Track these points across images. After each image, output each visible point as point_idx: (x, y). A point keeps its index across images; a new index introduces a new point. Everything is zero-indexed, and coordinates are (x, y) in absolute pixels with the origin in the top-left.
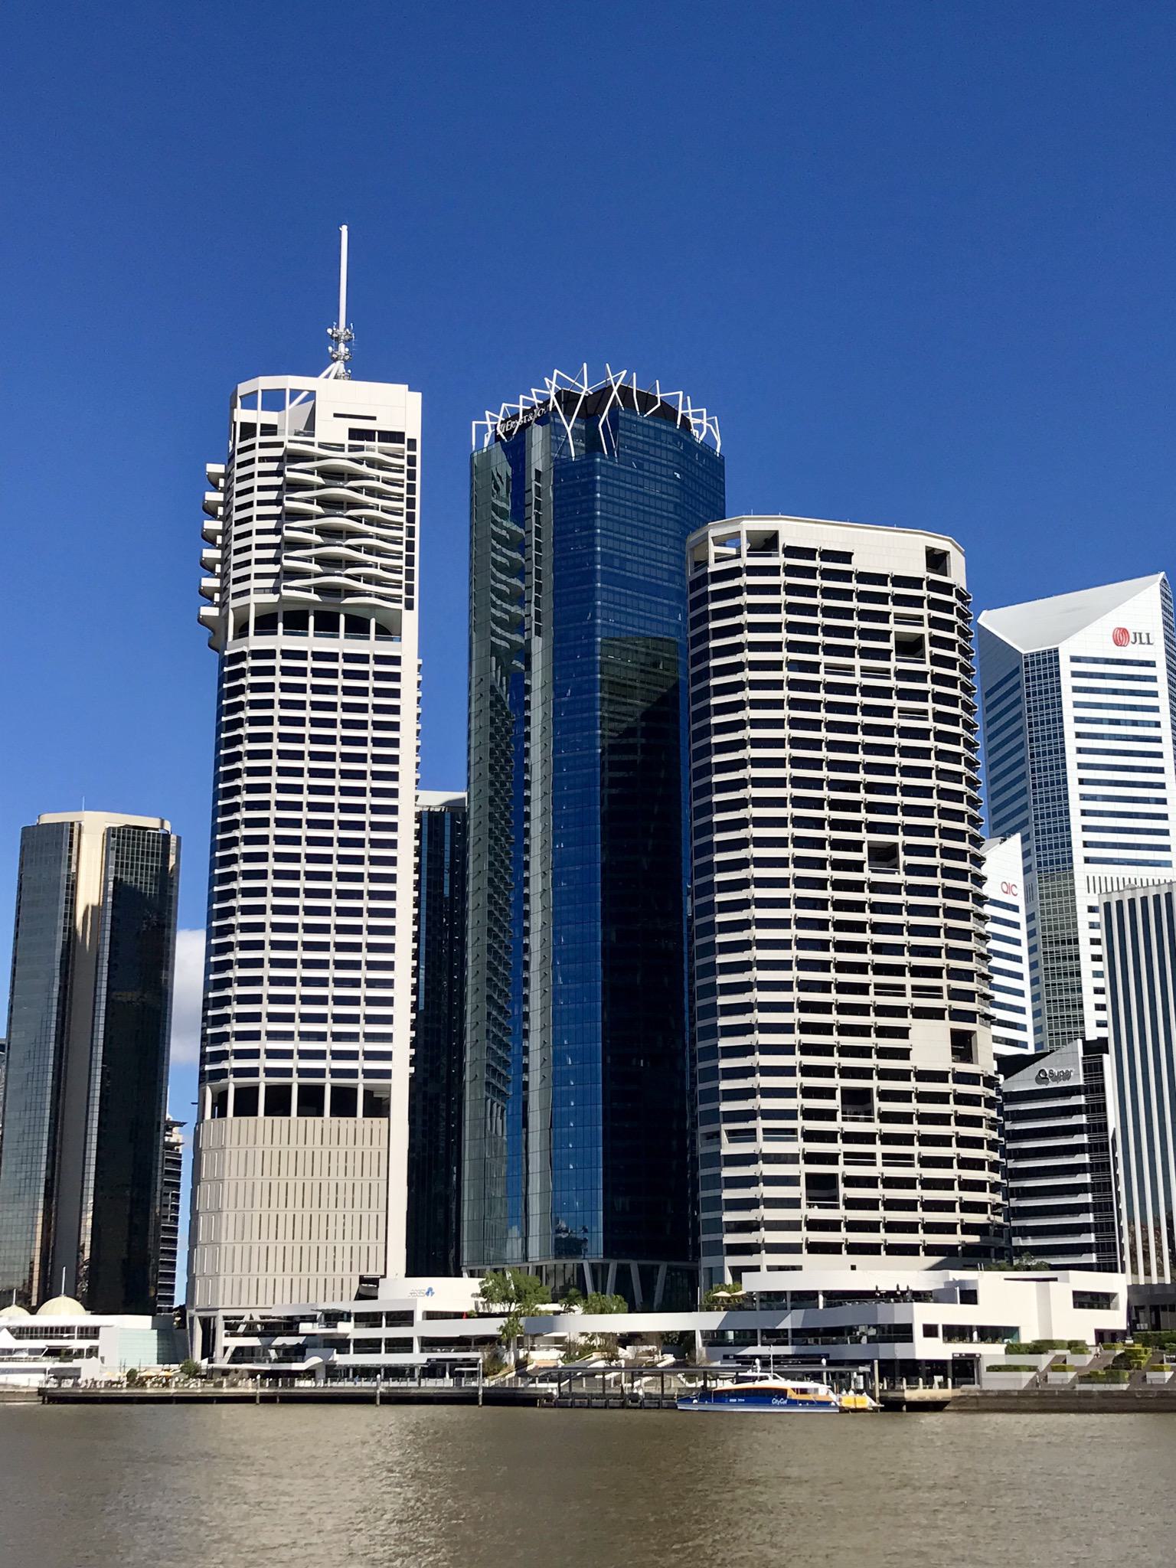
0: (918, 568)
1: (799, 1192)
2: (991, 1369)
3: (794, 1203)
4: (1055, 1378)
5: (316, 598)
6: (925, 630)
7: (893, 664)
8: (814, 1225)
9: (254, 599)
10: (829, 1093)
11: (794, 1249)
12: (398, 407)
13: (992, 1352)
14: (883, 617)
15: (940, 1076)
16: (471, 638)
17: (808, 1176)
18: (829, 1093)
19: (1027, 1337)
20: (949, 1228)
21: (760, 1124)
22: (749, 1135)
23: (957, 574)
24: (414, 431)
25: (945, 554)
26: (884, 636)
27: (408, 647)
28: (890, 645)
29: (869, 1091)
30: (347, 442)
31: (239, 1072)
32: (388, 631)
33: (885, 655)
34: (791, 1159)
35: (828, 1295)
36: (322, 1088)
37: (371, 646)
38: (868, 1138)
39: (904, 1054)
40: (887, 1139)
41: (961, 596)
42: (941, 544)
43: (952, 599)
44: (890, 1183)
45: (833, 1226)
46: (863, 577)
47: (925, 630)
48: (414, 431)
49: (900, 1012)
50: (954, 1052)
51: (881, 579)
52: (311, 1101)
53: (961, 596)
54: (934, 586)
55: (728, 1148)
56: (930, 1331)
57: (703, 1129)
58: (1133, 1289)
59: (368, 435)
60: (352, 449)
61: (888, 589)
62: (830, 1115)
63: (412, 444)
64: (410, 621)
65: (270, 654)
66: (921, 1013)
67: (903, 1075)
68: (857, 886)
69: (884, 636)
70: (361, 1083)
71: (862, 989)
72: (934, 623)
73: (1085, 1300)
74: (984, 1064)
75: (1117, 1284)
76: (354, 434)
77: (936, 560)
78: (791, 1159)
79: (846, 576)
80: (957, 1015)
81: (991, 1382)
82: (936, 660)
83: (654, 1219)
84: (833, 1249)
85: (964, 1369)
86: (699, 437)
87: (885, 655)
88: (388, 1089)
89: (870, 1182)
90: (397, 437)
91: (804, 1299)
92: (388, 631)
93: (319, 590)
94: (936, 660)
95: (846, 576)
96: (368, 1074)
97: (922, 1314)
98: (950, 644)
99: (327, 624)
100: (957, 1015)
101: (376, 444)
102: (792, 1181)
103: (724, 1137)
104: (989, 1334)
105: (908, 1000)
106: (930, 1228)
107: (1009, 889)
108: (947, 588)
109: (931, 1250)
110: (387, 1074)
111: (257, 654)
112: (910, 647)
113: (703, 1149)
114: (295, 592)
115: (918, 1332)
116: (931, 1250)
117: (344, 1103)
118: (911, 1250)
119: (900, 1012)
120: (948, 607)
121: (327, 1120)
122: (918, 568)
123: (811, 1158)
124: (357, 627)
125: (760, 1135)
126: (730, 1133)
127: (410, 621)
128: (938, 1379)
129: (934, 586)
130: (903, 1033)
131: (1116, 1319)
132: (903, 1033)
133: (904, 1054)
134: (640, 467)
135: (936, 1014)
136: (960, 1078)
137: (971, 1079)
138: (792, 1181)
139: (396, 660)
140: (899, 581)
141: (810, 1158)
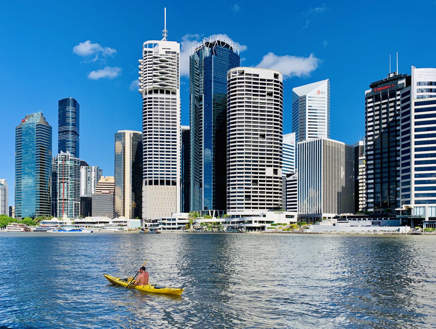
1: (244, 198)
2: (268, 228)
3: (243, 200)
5: (160, 87)
6: (273, 91)
8: (246, 204)
9: (148, 87)
10: (250, 181)
11: (243, 208)
14: (265, 88)
15: (271, 177)
16: (190, 94)
17: (245, 195)
18: (250, 181)
20: (271, 204)
21: (237, 186)
26: (265, 92)
27: (178, 96)
28: (266, 94)
29: (257, 180)
31: (149, 178)
33: (264, 96)
34: (243, 192)
36: (164, 180)
37: (171, 96)
38: (257, 189)
40: (260, 189)
41: (281, 83)
42: (277, 73)
43: (279, 84)
44: (260, 196)
45: (250, 204)
50: (274, 173)
52: (162, 183)
53: (281, 83)
54: (275, 81)
55: (231, 190)
57: (227, 187)
58: (298, 215)
62: (250, 185)
64: (178, 91)
65: (151, 98)
67: (264, 177)
68: (257, 142)
69: (265, 92)
70: (171, 180)
71: (257, 162)
72: (275, 89)
73: (287, 216)
74: (280, 175)
75: (296, 214)
78: (243, 192)
82: (275, 97)
83: (221, 204)
84: (250, 208)
85: (263, 228)
86: (235, 51)
87: (264, 96)
88: (176, 181)
89: (257, 196)
91: (238, 216)
92: (174, 93)
93: (160, 85)
94: (275, 97)
96: (172, 178)
97: (253, 219)
98: (278, 93)
99: (162, 92)
102: (243, 196)
103: (231, 189)
106: (267, 204)
108: (278, 82)
109: (267, 208)
110: (176, 178)
111: (149, 98)
112: (270, 94)
113: (227, 191)
114: (156, 85)
116: (267, 208)
117: (168, 183)
118: (264, 208)
120: (278, 86)
121: (165, 186)
123: (246, 192)
124: (168, 92)
125: (237, 188)
126: (232, 188)
128: (257, 230)
129: (275, 81)
134: (221, 58)
136: (275, 178)
137: (277, 178)
138: (243, 196)
140: (268, 80)
141: (246, 192)
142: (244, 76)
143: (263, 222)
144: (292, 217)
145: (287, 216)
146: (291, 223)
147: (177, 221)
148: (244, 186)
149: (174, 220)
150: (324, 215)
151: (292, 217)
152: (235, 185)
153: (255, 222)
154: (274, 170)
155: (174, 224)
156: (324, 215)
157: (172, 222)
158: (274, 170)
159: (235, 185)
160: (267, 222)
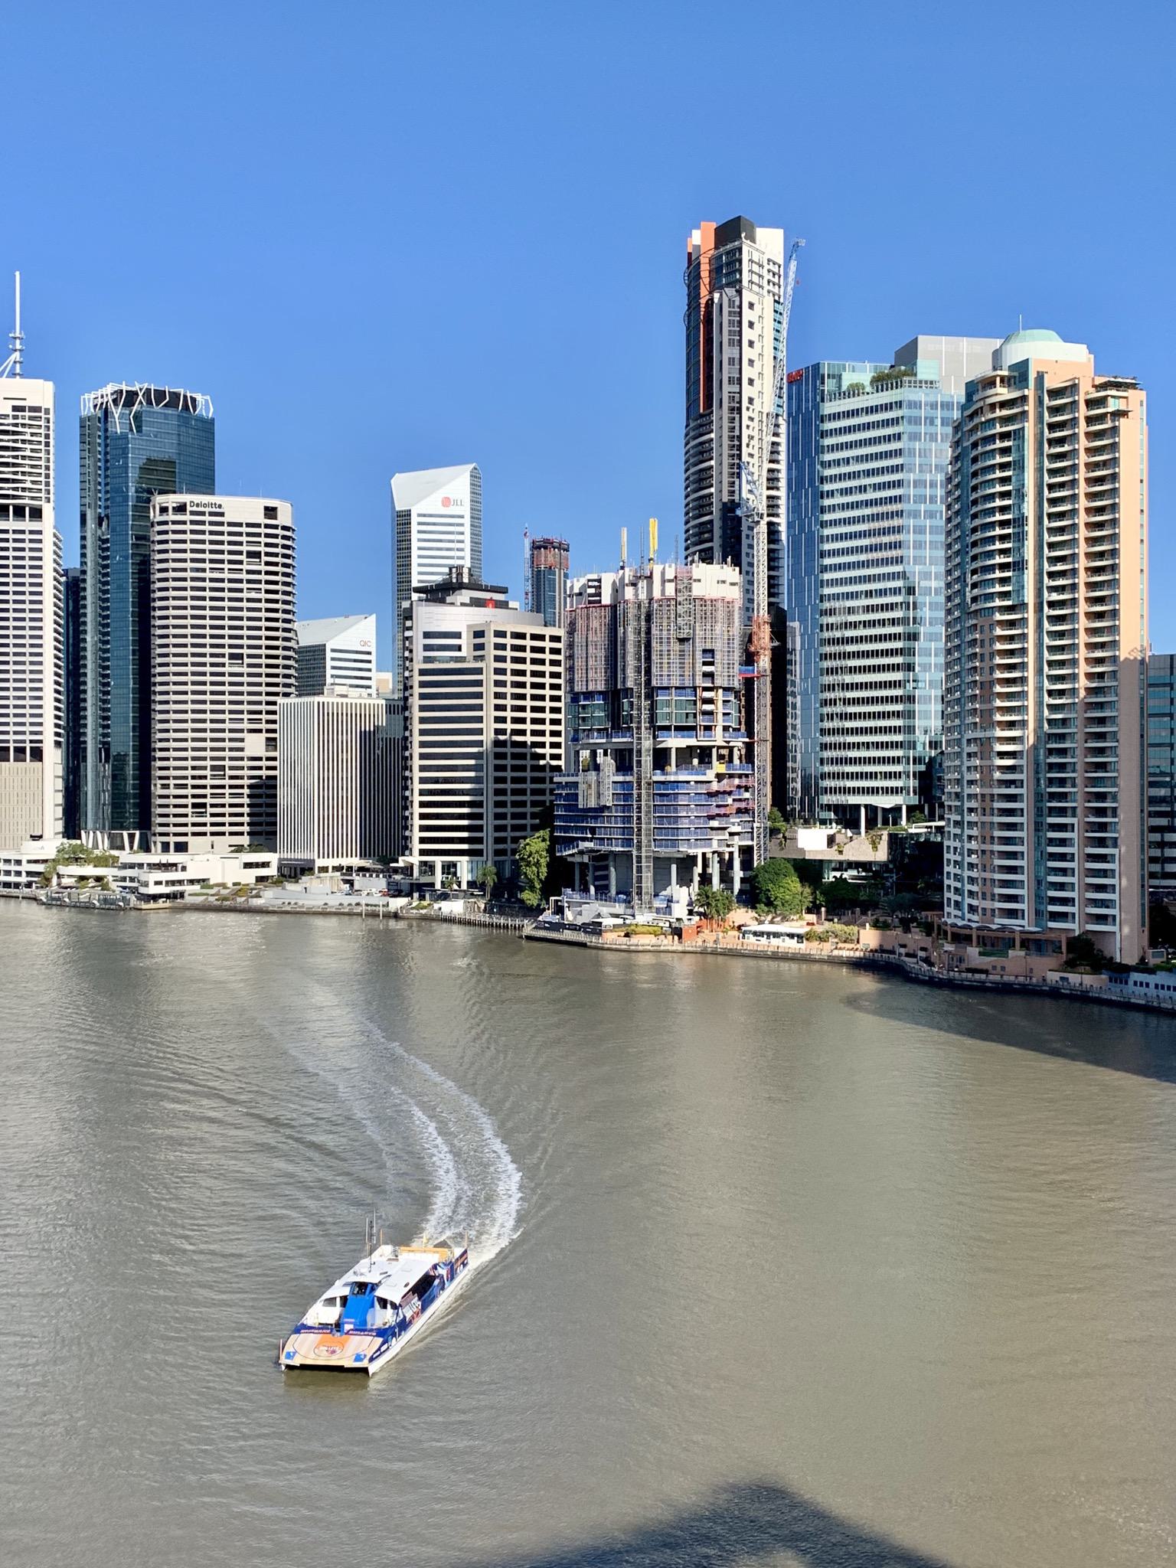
0: (261, 519)
4: (212, 899)
7: (245, 567)
12: (40, 392)
13: (197, 888)
14: (241, 544)
19: (212, 882)
22: (166, 786)
23: (284, 517)
24: (48, 402)
25: (274, 509)
26: (240, 553)
30: (11, 413)
32: (36, 514)
35: (149, 865)
39: (242, 750)
41: (285, 528)
46: (230, 524)
47: (262, 549)
48: (48, 402)
49: (242, 731)
51: (240, 525)
56: (158, 883)
58: (280, 860)
59: (22, 409)
60: (15, 417)
61: (244, 529)
63: (47, 411)
66: (251, 731)
73: (248, 865)
75: (272, 858)
76: (15, 408)
77: (271, 512)
79: (222, 524)
80: (268, 731)
81: (188, 900)
90: (37, 409)
95: (222, 524)
100: (268, 731)
101: (27, 414)
104: (192, 882)
105: (246, 725)
107: (365, 644)
110: (41, 741)
115: (151, 884)
119: (242, 731)
122: (261, 519)
127: (48, 511)
130: (242, 740)
131: (272, 871)
132: (242, 740)
133: (242, 750)
135: (260, 731)
139: (40, 532)
140: (248, 525)
142: (188, 517)
143: (180, 882)
144: (265, 865)
145: (248, 865)
146: (260, 879)
147: (25, 867)
148: (190, 782)
149: (18, 862)
150: (319, 863)
151: (265, 865)
152: (168, 778)
153: (158, 883)
154: (268, 739)
155: (18, 874)
156: (319, 863)
157: (13, 868)
158: (268, 739)
159: (168, 778)
160: (192, 882)
